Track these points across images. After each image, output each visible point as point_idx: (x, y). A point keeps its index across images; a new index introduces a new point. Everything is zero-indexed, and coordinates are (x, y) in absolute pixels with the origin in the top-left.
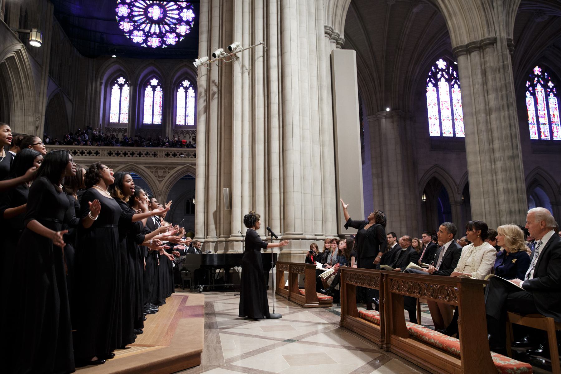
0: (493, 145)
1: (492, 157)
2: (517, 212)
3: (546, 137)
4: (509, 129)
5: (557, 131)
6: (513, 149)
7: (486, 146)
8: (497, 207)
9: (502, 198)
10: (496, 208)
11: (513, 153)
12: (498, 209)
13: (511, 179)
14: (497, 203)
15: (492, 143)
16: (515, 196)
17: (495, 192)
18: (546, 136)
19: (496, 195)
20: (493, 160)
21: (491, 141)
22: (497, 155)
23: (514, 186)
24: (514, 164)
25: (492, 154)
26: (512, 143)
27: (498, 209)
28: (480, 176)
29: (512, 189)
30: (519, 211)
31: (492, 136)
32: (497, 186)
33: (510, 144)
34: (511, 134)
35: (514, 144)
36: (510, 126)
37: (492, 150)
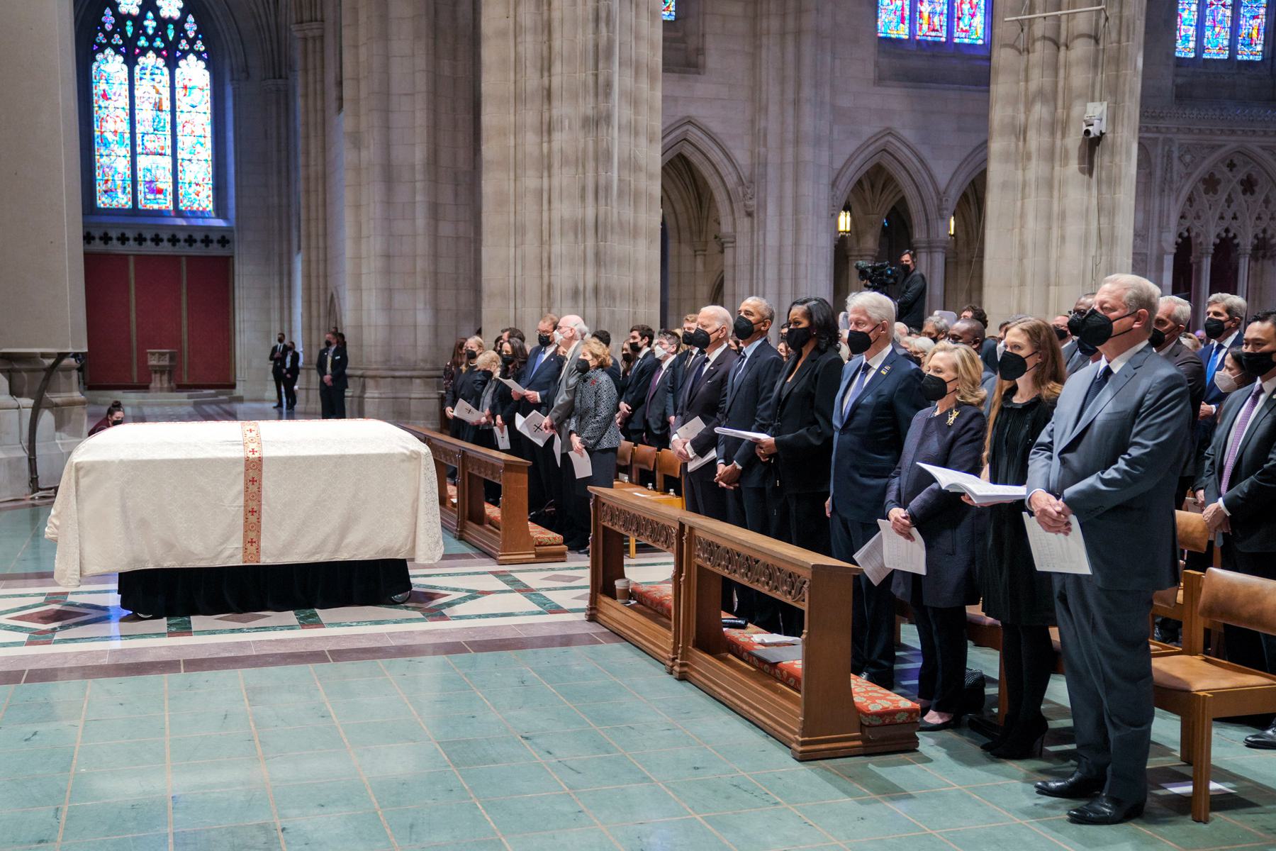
0: (550, 76)
1: (546, 116)
2: (589, 293)
3: (933, 34)
4: (591, 26)
5: (972, 12)
6: (596, 95)
7: (532, 80)
8: (545, 274)
9: (559, 247)
10: (542, 277)
11: (596, 107)
12: (546, 280)
13: (584, 189)
14: (545, 262)
15: (549, 70)
16: (590, 242)
17: (545, 226)
18: (934, 30)
19: (546, 237)
20: (545, 127)
21: (546, 66)
22: (560, 109)
23: (590, 212)
24: (596, 143)
25: (546, 107)
26: (596, 76)
27: (546, 280)
28: (512, 174)
29: (583, 221)
30: (596, 290)
31: (550, 47)
32: (550, 209)
33: (591, 80)
34: (596, 46)
35: (601, 79)
36: (597, 20)
37: (545, 93)
